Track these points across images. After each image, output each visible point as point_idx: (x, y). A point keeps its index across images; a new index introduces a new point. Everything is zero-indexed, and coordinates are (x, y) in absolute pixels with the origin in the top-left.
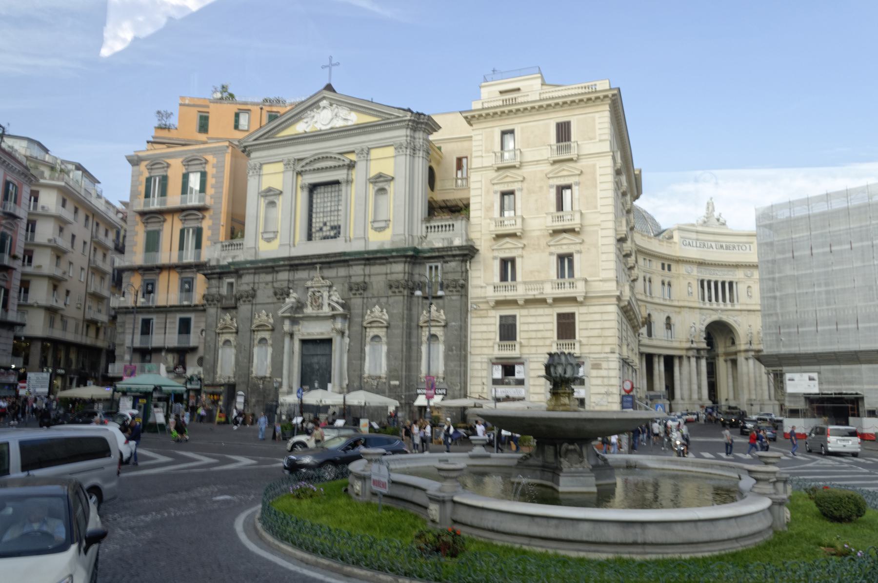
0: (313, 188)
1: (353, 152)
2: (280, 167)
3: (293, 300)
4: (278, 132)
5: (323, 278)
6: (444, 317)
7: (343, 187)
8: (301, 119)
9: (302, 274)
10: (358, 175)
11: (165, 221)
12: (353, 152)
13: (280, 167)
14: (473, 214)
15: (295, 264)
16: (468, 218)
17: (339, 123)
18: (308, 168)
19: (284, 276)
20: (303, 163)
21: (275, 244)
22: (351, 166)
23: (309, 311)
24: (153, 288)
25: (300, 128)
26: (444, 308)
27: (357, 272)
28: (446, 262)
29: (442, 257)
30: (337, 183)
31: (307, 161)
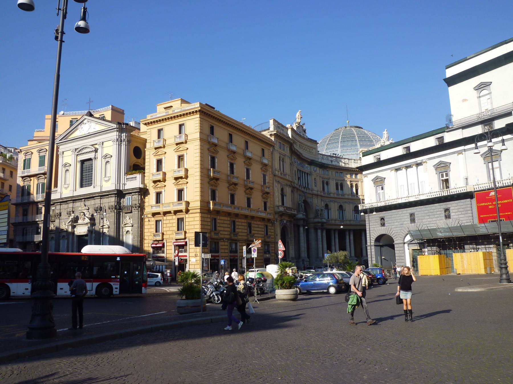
0: (83, 162)
1: (96, 144)
2: (70, 153)
3: (72, 217)
4: (69, 136)
5: (85, 206)
6: (132, 222)
7: (94, 160)
8: (77, 129)
9: (78, 204)
10: (99, 154)
11: (31, 180)
12: (96, 144)
13: (70, 153)
14: (146, 171)
15: (74, 200)
16: (144, 173)
17: (92, 131)
18: (80, 153)
19: (71, 205)
20: (78, 151)
21: (69, 189)
22: (96, 151)
23: (80, 221)
24: (27, 213)
25: (77, 134)
26: (132, 218)
27: (97, 202)
28: (133, 195)
29: (131, 193)
30: (90, 159)
31: (79, 149)
